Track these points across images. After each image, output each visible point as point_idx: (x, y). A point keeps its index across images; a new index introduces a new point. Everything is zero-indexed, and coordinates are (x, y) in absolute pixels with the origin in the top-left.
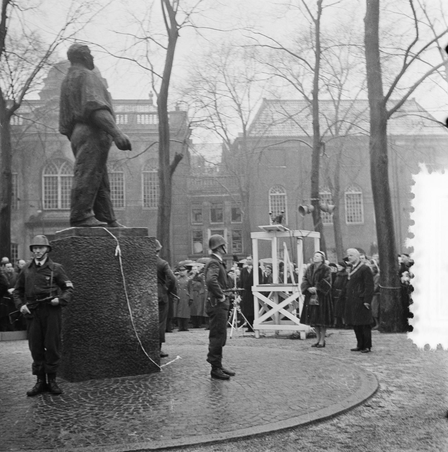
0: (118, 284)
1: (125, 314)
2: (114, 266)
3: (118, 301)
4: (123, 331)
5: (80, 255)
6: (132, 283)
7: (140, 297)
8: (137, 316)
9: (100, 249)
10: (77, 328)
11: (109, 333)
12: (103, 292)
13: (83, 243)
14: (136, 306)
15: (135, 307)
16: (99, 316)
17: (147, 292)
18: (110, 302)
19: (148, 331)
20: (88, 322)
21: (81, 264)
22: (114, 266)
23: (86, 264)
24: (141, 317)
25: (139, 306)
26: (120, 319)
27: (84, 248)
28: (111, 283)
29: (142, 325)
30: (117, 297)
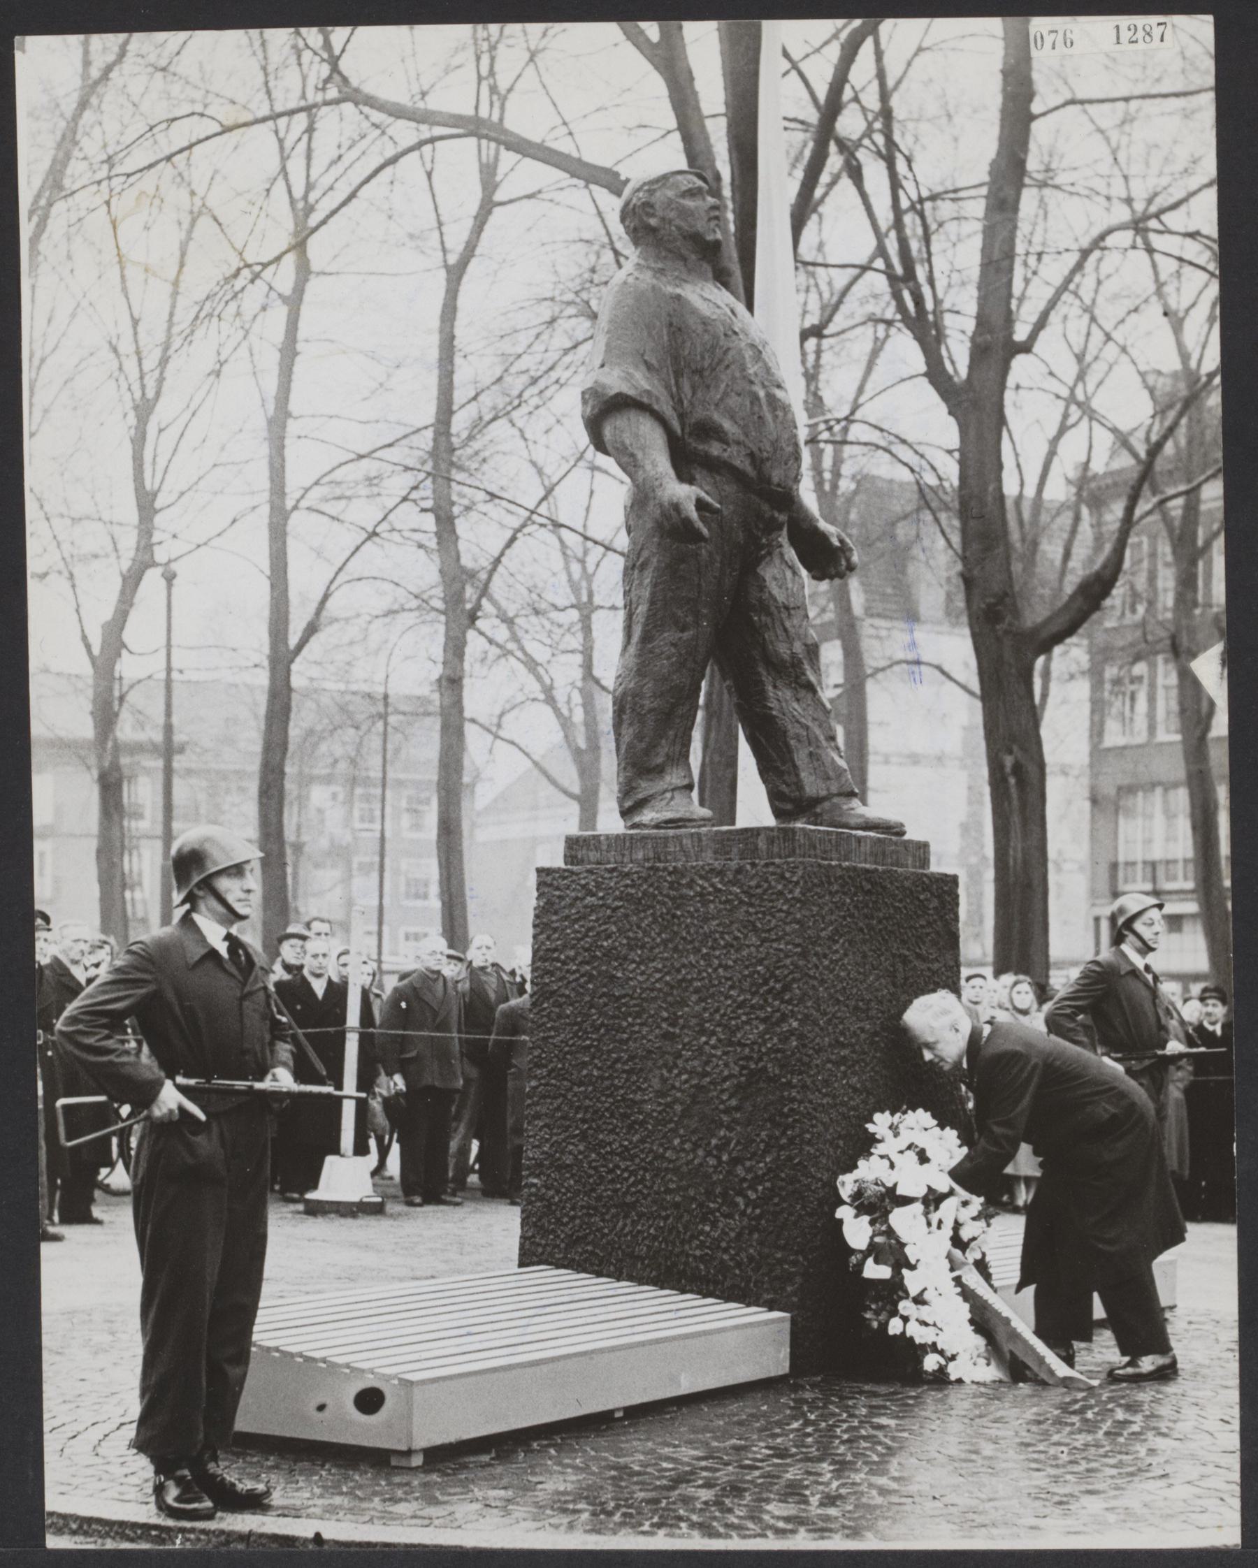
0: (667, 1036)
1: (687, 1146)
2: (657, 970)
3: (661, 1094)
4: (676, 1206)
5: (555, 930)
6: (713, 1033)
7: (739, 1086)
8: (725, 1158)
9: (615, 909)
10: (538, 1176)
11: (633, 1206)
12: (617, 1060)
13: (568, 887)
14: (725, 1118)
15: (721, 1125)
16: (602, 1144)
17: (764, 1069)
18: (638, 1097)
19: (760, 1217)
20: (569, 1160)
21: (558, 960)
22: (657, 970)
23: (573, 959)
24: (735, 1161)
25: (734, 1121)
26: (670, 1161)
27: (571, 905)
28: (645, 1030)
29: (741, 1193)
30: (664, 1080)
